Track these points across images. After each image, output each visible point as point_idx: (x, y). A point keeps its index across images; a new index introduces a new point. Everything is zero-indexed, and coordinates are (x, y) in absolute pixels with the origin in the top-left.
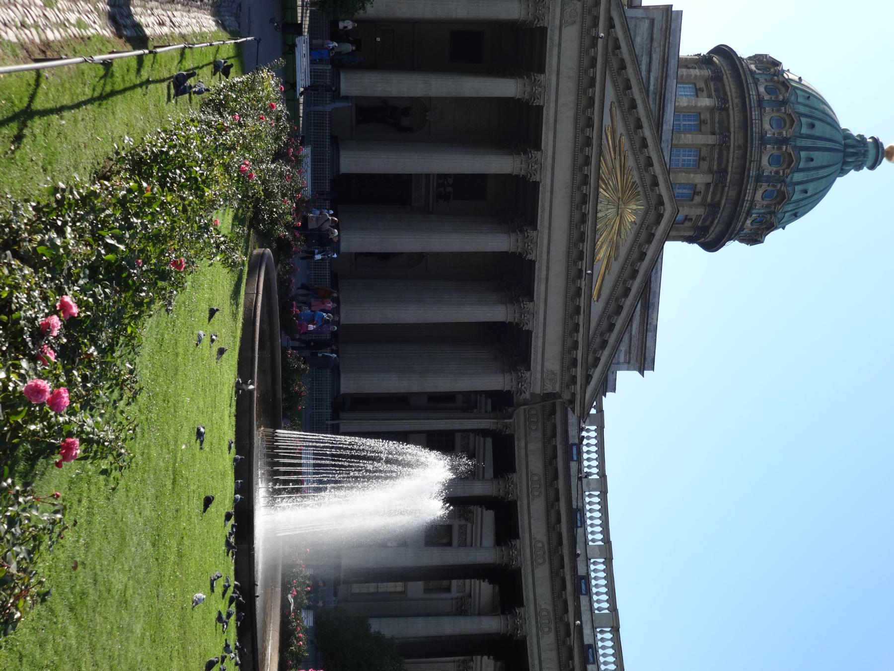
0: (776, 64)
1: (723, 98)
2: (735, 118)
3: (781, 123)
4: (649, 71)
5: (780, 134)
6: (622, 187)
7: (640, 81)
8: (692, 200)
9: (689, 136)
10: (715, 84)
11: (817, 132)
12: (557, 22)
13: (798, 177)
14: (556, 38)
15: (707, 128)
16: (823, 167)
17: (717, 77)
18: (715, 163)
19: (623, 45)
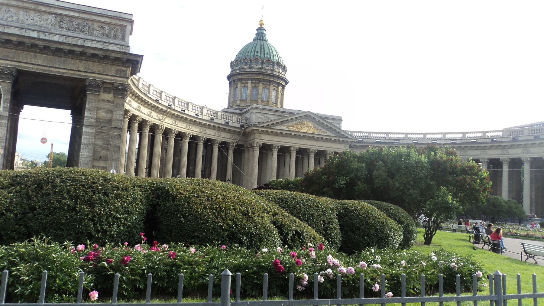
0: (236, 60)
2: (255, 77)
3: (257, 62)
4: (268, 114)
5: (260, 63)
6: (301, 125)
7: (278, 119)
8: (276, 91)
11: (259, 51)
12: (261, 140)
13: (272, 58)
14: (264, 141)
15: (257, 85)
16: (269, 49)
18: (267, 83)
19: (268, 124)
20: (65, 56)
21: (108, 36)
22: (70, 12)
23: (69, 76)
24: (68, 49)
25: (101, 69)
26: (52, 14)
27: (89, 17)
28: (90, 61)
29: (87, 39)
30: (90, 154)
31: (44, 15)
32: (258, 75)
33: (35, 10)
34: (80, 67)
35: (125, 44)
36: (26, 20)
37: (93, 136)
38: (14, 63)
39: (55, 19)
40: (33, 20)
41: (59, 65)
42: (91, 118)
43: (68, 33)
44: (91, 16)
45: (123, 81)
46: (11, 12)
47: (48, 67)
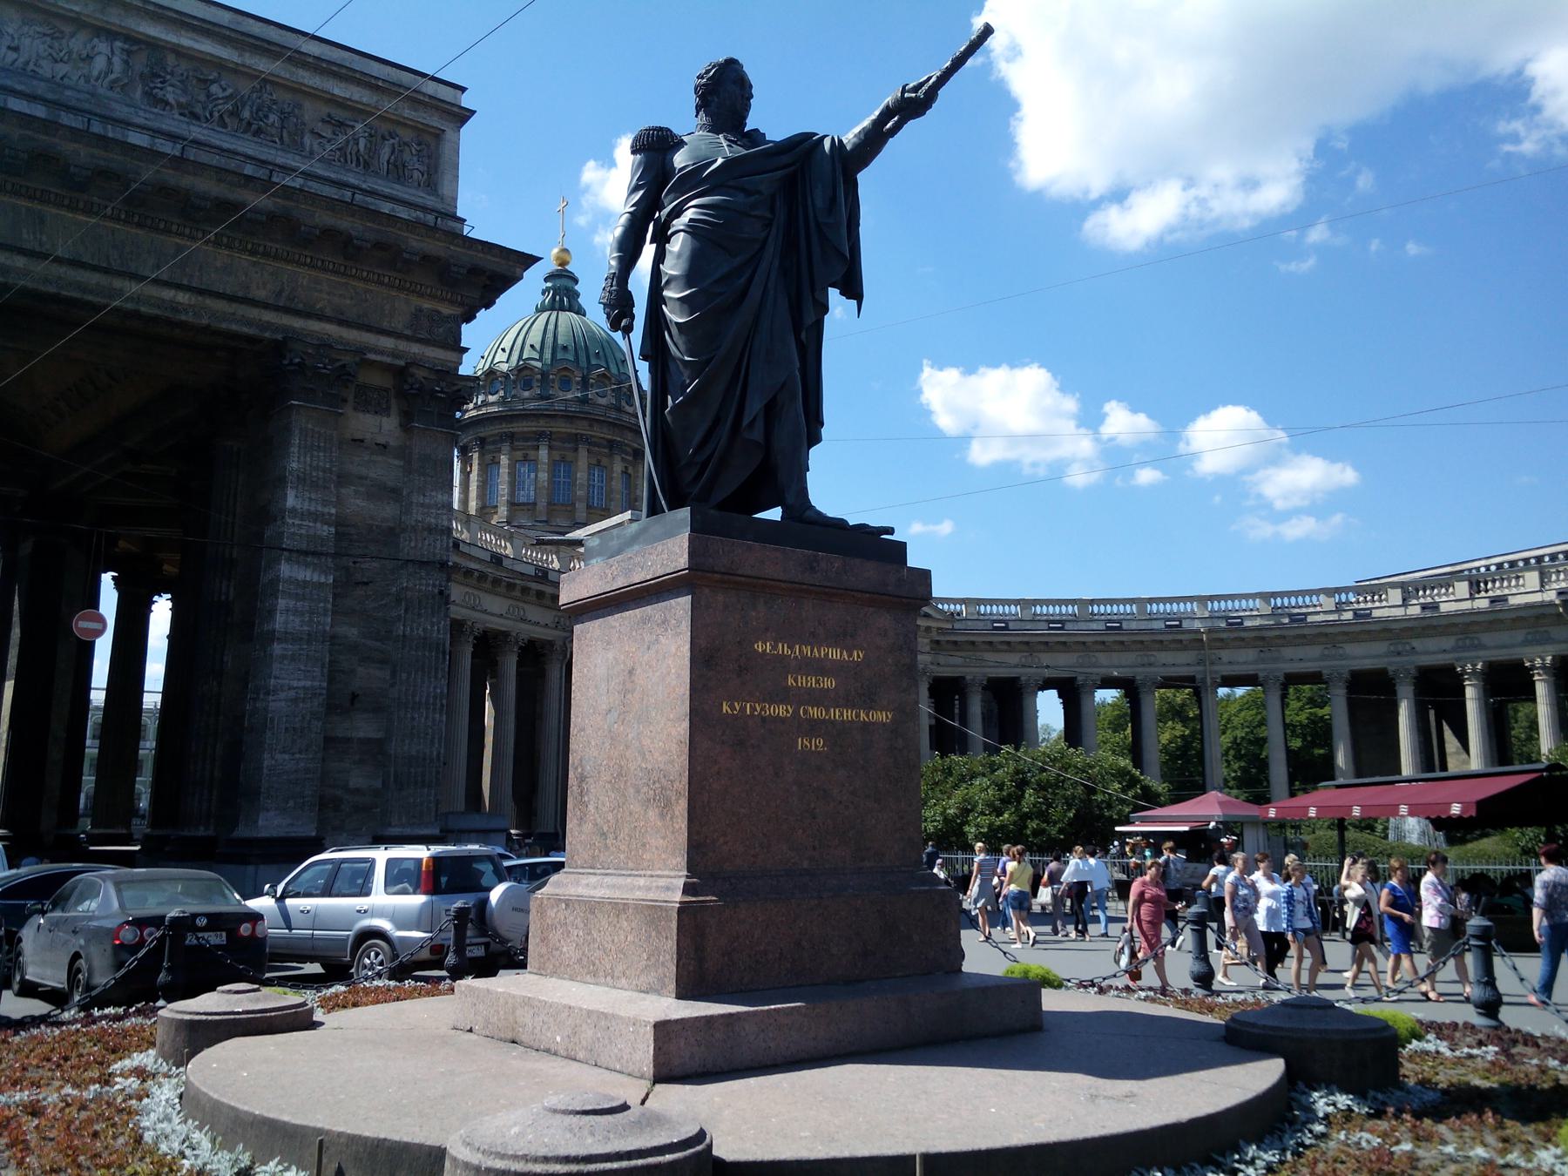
1: (540, 436)
5: (578, 383)
8: (630, 475)
9: (578, 475)
10: (518, 440)
13: (614, 370)
15: (570, 456)
17: (511, 437)
20: (187, 231)
21: (367, 165)
22: (194, 35)
23: (205, 321)
25: (348, 302)
26: (111, 34)
27: (282, 74)
28: (299, 264)
30: (316, 684)
31: (72, 35)
32: (571, 423)
35: (439, 206)
37: (326, 601)
39: (126, 62)
40: (16, 49)
42: (316, 517)
43: (192, 128)
47: (106, 271)
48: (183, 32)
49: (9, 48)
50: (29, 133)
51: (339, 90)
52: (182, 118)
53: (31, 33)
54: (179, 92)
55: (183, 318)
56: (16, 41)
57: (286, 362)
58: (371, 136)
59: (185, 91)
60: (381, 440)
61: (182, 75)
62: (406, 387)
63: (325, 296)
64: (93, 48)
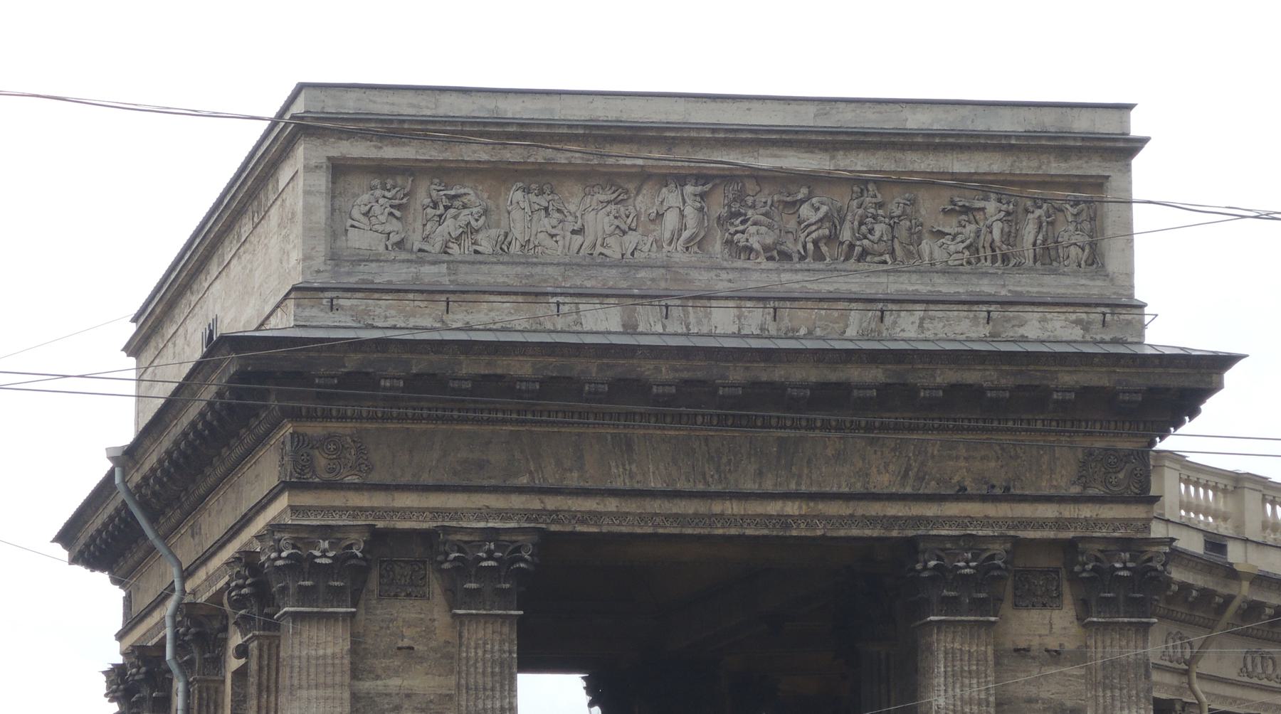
21: (1005, 259)
23: (819, 533)
24: (813, 379)
26: (680, 179)
27: (889, 166)
29: (894, 301)
33: (586, 176)
34: (874, 470)
36: (549, 242)
38: (517, 502)
39: (701, 210)
41: (760, 474)
43: (785, 277)
44: (899, 155)
45: (1127, 523)
46: (465, 206)
48: (761, 151)
49: (574, 232)
50: (605, 361)
51: (959, 164)
52: (771, 265)
53: (594, 203)
54: (763, 229)
55: (794, 533)
56: (580, 222)
57: (919, 566)
58: (1008, 213)
59: (770, 227)
60: (1053, 644)
61: (765, 203)
62: (1077, 568)
63: (963, 464)
64: (662, 202)
